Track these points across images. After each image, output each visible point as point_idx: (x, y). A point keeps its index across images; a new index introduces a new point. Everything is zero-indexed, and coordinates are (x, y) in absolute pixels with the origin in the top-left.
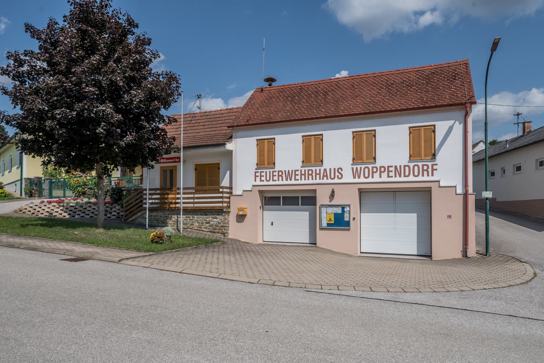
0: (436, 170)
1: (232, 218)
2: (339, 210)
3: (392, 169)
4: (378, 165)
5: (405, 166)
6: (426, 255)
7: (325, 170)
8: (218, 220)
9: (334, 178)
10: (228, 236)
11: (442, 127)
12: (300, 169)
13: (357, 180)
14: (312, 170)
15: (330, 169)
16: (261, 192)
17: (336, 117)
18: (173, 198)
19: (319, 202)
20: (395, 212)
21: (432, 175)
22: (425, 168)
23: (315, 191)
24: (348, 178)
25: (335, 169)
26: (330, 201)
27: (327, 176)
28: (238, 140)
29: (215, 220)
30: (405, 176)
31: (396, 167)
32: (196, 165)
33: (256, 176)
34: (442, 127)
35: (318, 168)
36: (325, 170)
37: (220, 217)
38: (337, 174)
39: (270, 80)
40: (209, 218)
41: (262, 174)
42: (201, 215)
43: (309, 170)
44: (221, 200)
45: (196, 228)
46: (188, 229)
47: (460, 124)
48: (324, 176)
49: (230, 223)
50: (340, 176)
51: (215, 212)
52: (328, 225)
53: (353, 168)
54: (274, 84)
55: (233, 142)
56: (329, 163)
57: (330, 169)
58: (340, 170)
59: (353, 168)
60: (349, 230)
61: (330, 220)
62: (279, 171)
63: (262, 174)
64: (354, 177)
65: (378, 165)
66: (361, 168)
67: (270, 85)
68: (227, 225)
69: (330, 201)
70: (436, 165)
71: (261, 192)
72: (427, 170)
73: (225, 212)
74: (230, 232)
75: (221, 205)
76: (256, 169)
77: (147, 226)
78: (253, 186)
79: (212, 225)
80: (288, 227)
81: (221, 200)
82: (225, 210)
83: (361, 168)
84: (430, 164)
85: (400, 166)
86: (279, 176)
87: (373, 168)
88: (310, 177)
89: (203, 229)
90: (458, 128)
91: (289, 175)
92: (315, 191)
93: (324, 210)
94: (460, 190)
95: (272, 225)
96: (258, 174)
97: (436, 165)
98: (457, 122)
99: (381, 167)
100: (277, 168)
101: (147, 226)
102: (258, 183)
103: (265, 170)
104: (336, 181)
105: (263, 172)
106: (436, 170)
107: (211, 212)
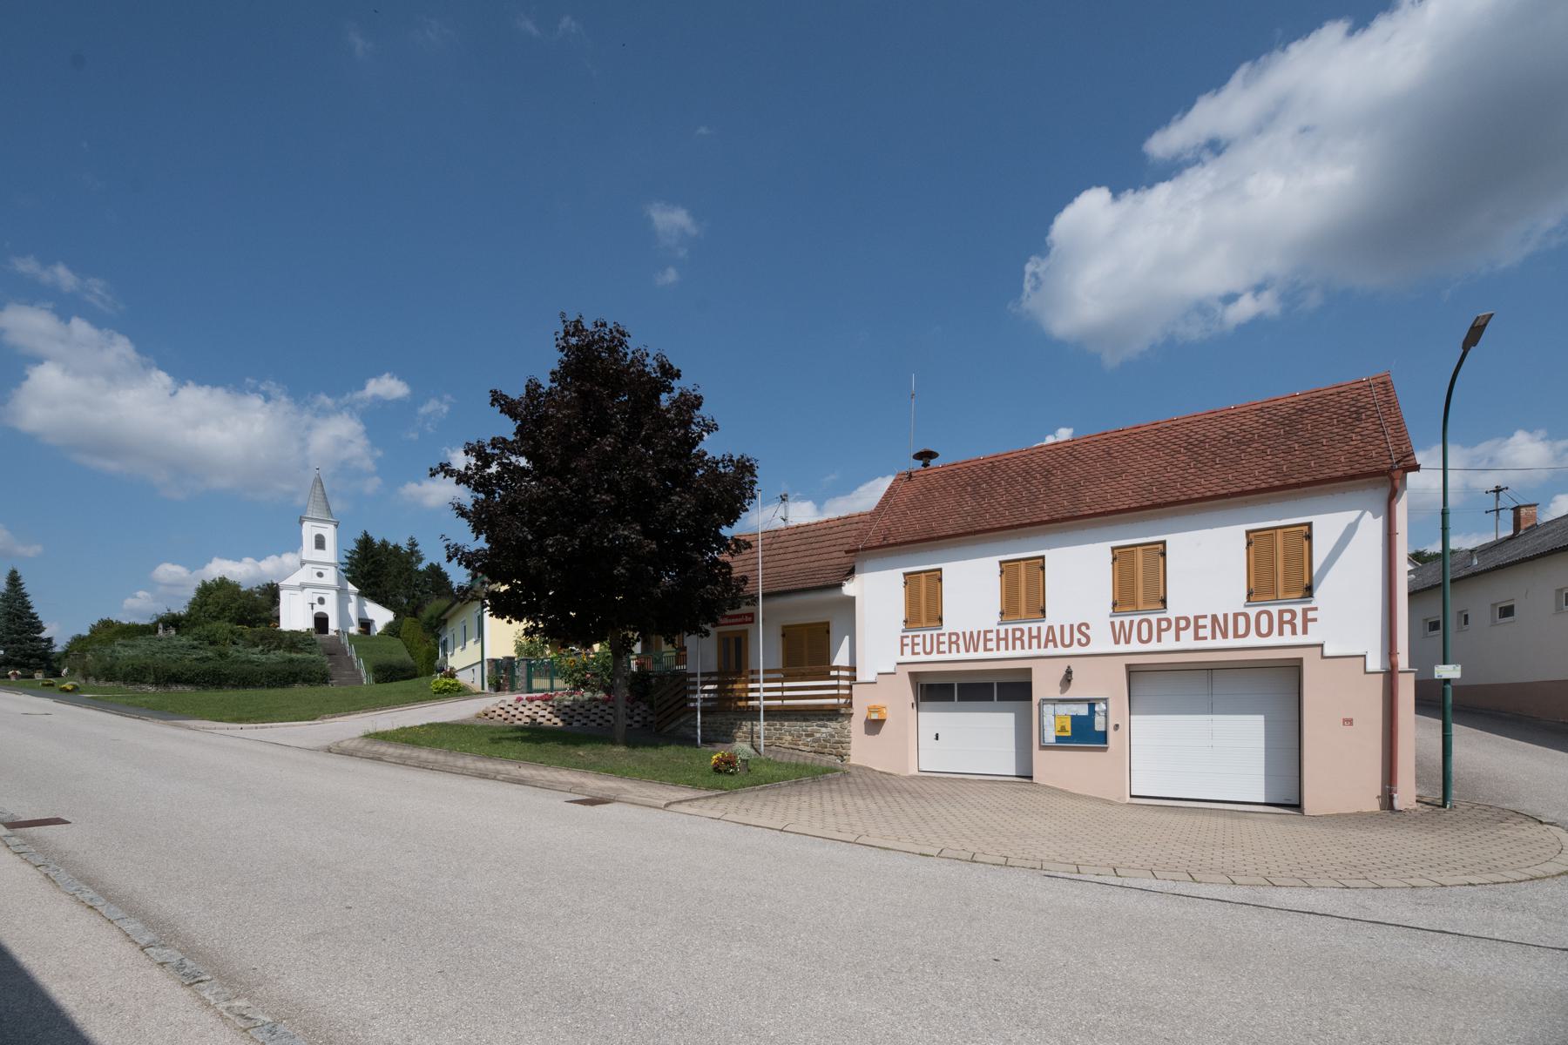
1: (856, 725)
2: (1083, 710)
3: (1208, 622)
5: (1236, 616)
7: (1051, 628)
9: (1071, 644)
11: (1327, 525)
12: (995, 628)
14: (1022, 631)
16: (913, 675)
17: (1074, 520)
19: (1037, 695)
21: (1305, 631)
23: (1029, 671)
24: (1102, 641)
26: (1062, 692)
29: (824, 730)
30: (1236, 635)
31: (1214, 618)
32: (784, 627)
33: (903, 645)
35: (1034, 626)
36: (1051, 628)
37: (833, 724)
38: (1077, 635)
39: (926, 456)
40: (813, 726)
47: (1375, 517)
48: (1047, 641)
50: (1084, 640)
52: (1058, 739)
53: (1113, 624)
54: (933, 463)
59: (1113, 624)
61: (1063, 729)
64: (1117, 642)
67: (925, 465)
69: (1062, 692)
71: (913, 675)
74: (851, 752)
75: (835, 701)
79: (818, 740)
84: (1298, 609)
85: (1226, 616)
86: (951, 643)
90: (1372, 527)
92: (1029, 671)
93: (1048, 709)
96: (906, 641)
98: (1368, 515)
99: (1178, 619)
100: (947, 627)
102: (908, 657)
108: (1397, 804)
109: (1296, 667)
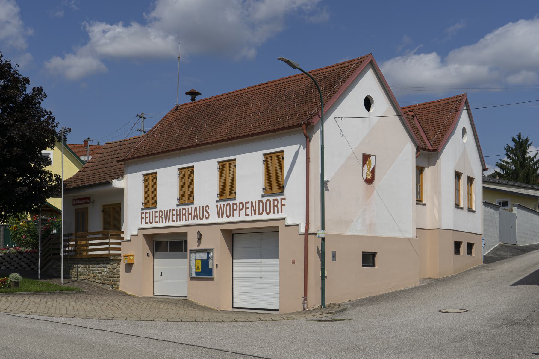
0: (284, 205)
1: (122, 267)
2: (204, 256)
3: (249, 205)
4: (237, 201)
5: (259, 201)
6: (304, 310)
7: (196, 208)
8: (107, 269)
10: (118, 288)
11: (289, 151)
12: (176, 208)
13: (221, 220)
15: (200, 207)
16: (145, 235)
17: (202, 146)
18: (84, 245)
19: (190, 247)
20: (262, 258)
21: (281, 212)
22: (276, 203)
23: (186, 234)
25: (203, 207)
26: (198, 246)
27: (197, 216)
28: (128, 175)
29: (107, 269)
30: (259, 214)
31: (252, 202)
32: (104, 206)
33: (142, 218)
34: (289, 151)
35: (190, 207)
36: (196, 208)
37: (109, 266)
38: (205, 213)
39: (193, 94)
40: (100, 267)
41: (148, 215)
42: (95, 264)
43: (183, 209)
44: (107, 246)
45: (91, 279)
46: (86, 281)
47: (304, 149)
48: (195, 216)
49: (120, 273)
50: (207, 216)
51: (105, 261)
52: (197, 273)
53: (217, 205)
54: (198, 98)
55: (125, 178)
56: (199, 200)
57: (200, 207)
58: (207, 208)
59: (217, 205)
60: (212, 279)
61: (198, 268)
62: (160, 211)
63: (148, 215)
64: (219, 217)
65: (237, 201)
66: (224, 205)
67: (193, 99)
68: (117, 276)
69: (198, 246)
70: (284, 199)
71: (145, 235)
72: (277, 206)
73: (112, 260)
74: (121, 283)
75: (106, 252)
76: (142, 209)
77: (39, 277)
78: (139, 229)
79: (102, 276)
80: (171, 276)
81: (107, 246)
82: (111, 258)
83: (224, 205)
84: (279, 198)
85: (255, 202)
86: (160, 217)
87: (233, 204)
88: (196, 218)
89: (97, 281)
90: (303, 152)
91: (254, 207)
92: (186, 234)
93: (193, 255)
94: (302, 231)
95: (161, 273)
96: (144, 215)
97: (284, 199)
98: (302, 147)
99: (240, 203)
100: (158, 209)
101: (39, 277)
102: (144, 226)
103: (148, 211)
104: (205, 221)
105: (147, 213)
106: (284, 205)
107: (102, 261)
108: (327, 303)
109: (275, 231)
